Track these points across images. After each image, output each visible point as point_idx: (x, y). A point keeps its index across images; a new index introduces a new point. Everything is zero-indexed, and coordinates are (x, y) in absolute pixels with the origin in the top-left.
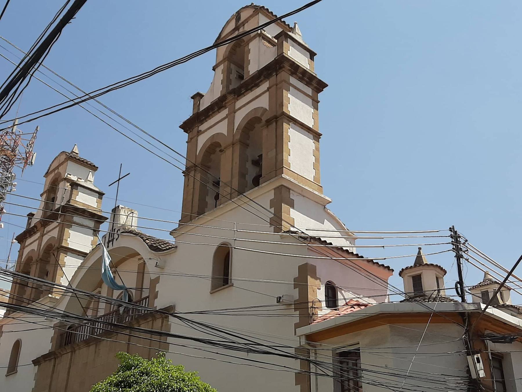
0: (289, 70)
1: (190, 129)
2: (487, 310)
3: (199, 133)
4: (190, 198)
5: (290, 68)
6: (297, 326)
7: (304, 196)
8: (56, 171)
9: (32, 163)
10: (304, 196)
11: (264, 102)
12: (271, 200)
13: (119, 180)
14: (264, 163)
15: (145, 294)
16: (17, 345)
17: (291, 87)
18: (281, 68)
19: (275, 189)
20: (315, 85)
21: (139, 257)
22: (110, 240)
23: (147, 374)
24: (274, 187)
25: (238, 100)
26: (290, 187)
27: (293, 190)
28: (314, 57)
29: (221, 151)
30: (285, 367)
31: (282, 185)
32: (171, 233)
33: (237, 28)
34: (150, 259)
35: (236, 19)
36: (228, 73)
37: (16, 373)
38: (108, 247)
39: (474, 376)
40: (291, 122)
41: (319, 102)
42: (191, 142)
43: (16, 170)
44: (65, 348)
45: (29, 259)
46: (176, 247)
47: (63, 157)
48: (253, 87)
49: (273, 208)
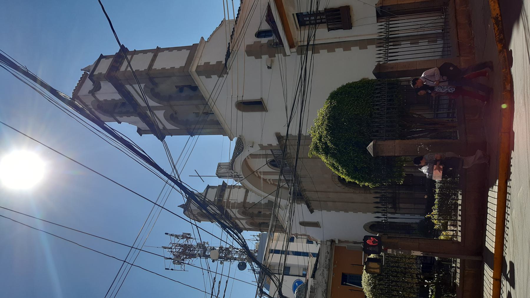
0: (116, 71)
3: (164, 128)
5: (115, 71)
6: (285, 55)
7: (201, 56)
8: (196, 215)
10: (201, 56)
12: (207, 77)
13: (199, 176)
14: (181, 84)
15: (269, 152)
16: (303, 224)
19: (199, 76)
22: (237, 177)
24: (197, 76)
25: (140, 105)
26: (196, 65)
27: (198, 64)
29: (176, 113)
30: (311, 60)
31: (196, 70)
32: (231, 140)
34: (249, 151)
37: (318, 222)
38: (242, 178)
40: (152, 68)
41: (135, 50)
42: (172, 133)
43: (194, 243)
44: (304, 195)
45: (252, 224)
46: (240, 136)
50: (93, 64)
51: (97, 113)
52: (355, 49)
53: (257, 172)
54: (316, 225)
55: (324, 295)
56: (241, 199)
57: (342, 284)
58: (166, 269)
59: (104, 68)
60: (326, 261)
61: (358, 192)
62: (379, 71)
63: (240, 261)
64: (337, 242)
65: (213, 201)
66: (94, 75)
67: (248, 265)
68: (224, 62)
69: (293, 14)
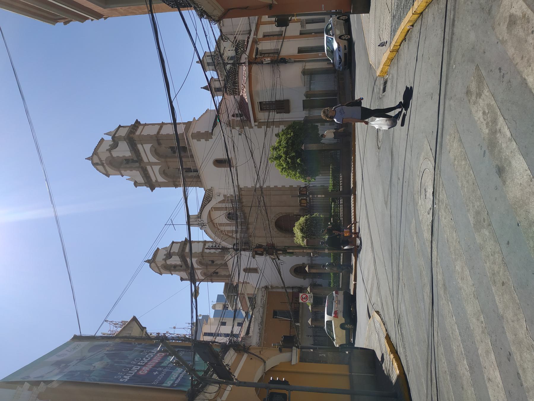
2: (248, 55)
3: (156, 181)
5: (132, 135)
8: (160, 268)
17: (142, 134)
25: (144, 161)
29: (169, 168)
33: (103, 165)
35: (97, 165)
36: (126, 169)
38: (206, 226)
39: (270, 62)
40: (159, 134)
42: (161, 185)
47: (153, 264)
48: (139, 153)
49: (201, 140)
51: (107, 167)
54: (255, 270)
55: (260, 326)
59: (123, 133)
60: (261, 302)
61: (288, 237)
64: (270, 287)
65: (177, 252)
66: (115, 137)
68: (210, 131)
69: (258, 102)
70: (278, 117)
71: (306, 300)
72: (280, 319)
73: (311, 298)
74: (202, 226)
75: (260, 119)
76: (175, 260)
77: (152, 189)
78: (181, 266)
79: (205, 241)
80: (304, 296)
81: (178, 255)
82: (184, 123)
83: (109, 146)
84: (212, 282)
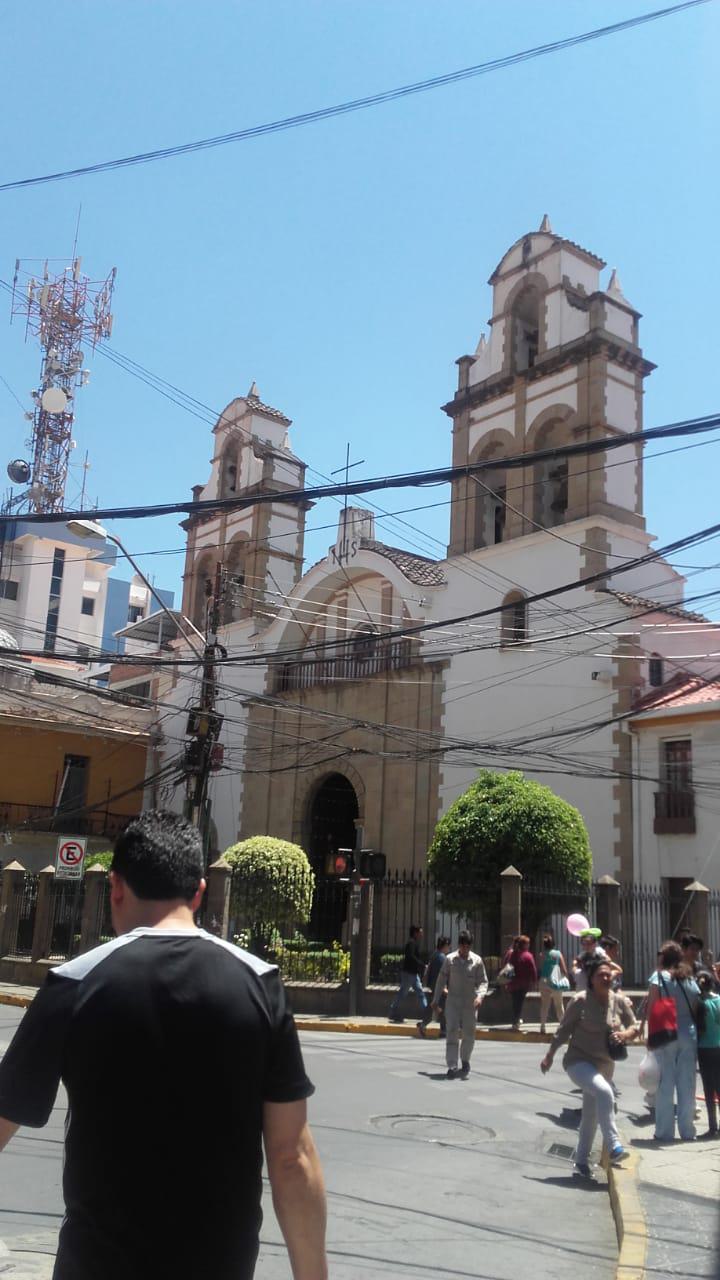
0: (607, 355)
1: (456, 413)
3: (471, 421)
4: (463, 518)
9: (109, 333)
11: (569, 398)
17: (609, 381)
18: (595, 353)
19: (587, 531)
20: (640, 369)
21: (383, 579)
23: (513, 793)
25: (529, 385)
28: (640, 321)
33: (525, 265)
36: (511, 333)
38: (340, 564)
43: (84, 347)
47: (242, 408)
50: (624, 300)
52: (615, 835)
53: (346, 594)
56: (275, 543)
57: (67, 757)
58: (18, 262)
59: (616, 325)
62: (603, 889)
63: (32, 466)
65: (274, 478)
67: (21, 488)
69: (689, 735)
70: (645, 796)
71: (65, 858)
72: (60, 774)
73: (71, 874)
74: (339, 553)
75: (639, 740)
76: (251, 469)
77: (451, 409)
78: (233, 489)
79: (301, 561)
80: (77, 852)
81: (263, 481)
82: (639, 507)
83: (579, 285)
84: (185, 577)
